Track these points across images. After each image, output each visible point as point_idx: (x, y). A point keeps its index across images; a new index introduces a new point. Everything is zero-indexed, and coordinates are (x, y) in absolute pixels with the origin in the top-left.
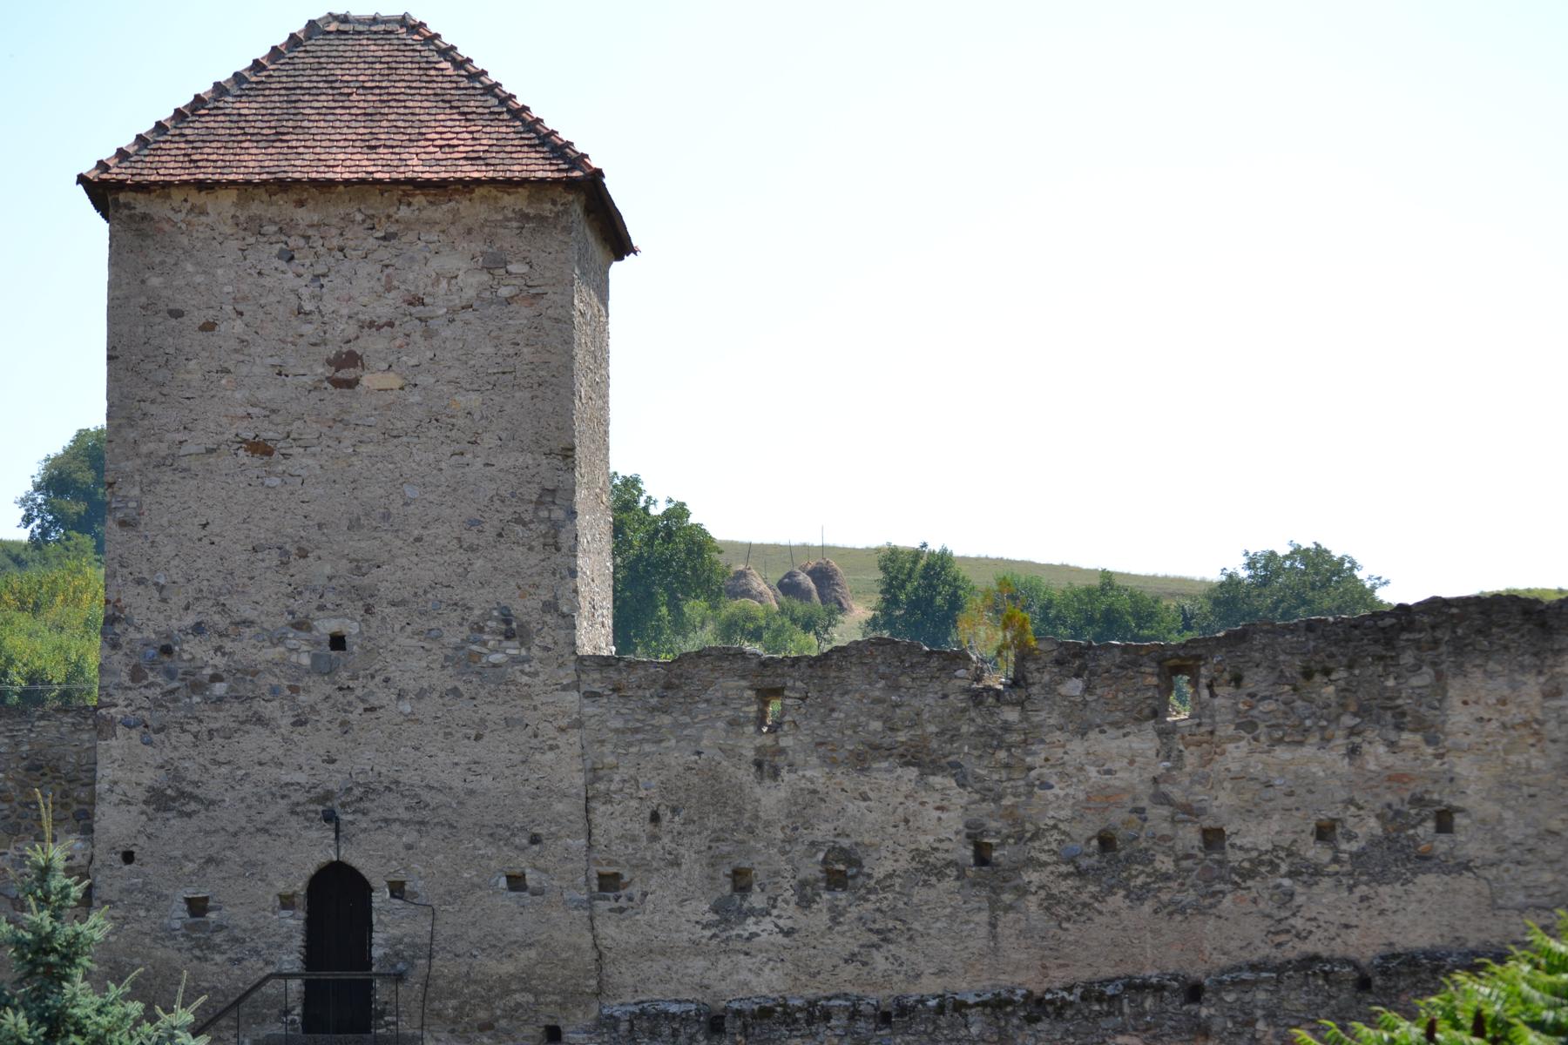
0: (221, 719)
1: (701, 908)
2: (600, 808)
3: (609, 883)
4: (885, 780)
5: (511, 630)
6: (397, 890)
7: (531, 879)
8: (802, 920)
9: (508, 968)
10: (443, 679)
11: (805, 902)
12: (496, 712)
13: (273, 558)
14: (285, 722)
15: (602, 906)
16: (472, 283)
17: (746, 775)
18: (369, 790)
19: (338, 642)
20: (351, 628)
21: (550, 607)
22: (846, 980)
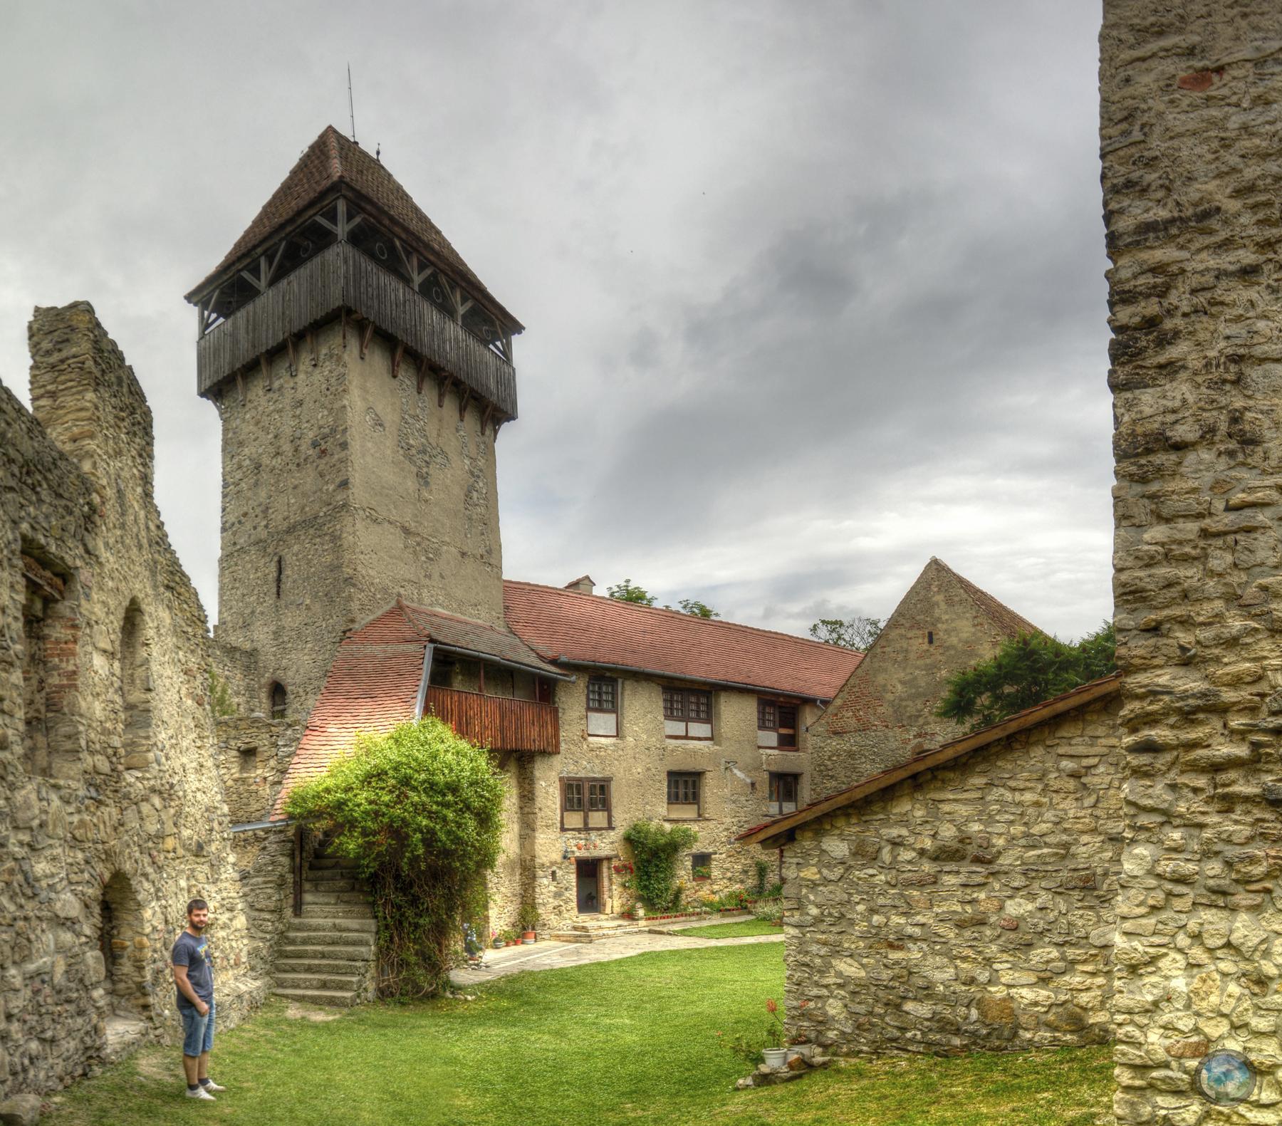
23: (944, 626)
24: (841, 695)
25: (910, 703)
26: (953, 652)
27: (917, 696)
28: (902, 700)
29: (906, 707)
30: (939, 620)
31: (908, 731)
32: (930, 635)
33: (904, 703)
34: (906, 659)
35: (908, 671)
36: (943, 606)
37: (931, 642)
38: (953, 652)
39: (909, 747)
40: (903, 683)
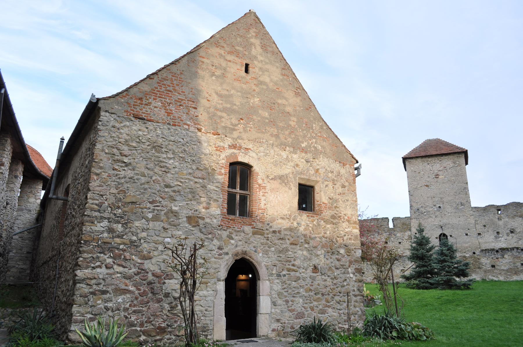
0: (426, 217)
1: (493, 237)
2: (477, 225)
3: (479, 234)
4: (517, 219)
5: (462, 204)
6: (451, 236)
7: (469, 234)
8: (507, 238)
9: (467, 245)
10: (454, 211)
11: (508, 236)
12: (461, 214)
13: (430, 198)
14: (434, 217)
15: (479, 237)
16: (452, 165)
17: (497, 220)
18: (446, 224)
19: (440, 207)
20: (441, 206)
21: (467, 201)
22: (515, 245)
23: (260, 65)
24: (148, 81)
25: (224, 115)
26: (265, 87)
27: (230, 111)
28: (217, 110)
29: (221, 117)
30: (255, 57)
31: (223, 141)
32: (247, 66)
33: (219, 113)
34: (223, 76)
35: (225, 86)
36: (259, 49)
37: (247, 71)
38: (265, 87)
39: (223, 156)
40: (220, 96)
